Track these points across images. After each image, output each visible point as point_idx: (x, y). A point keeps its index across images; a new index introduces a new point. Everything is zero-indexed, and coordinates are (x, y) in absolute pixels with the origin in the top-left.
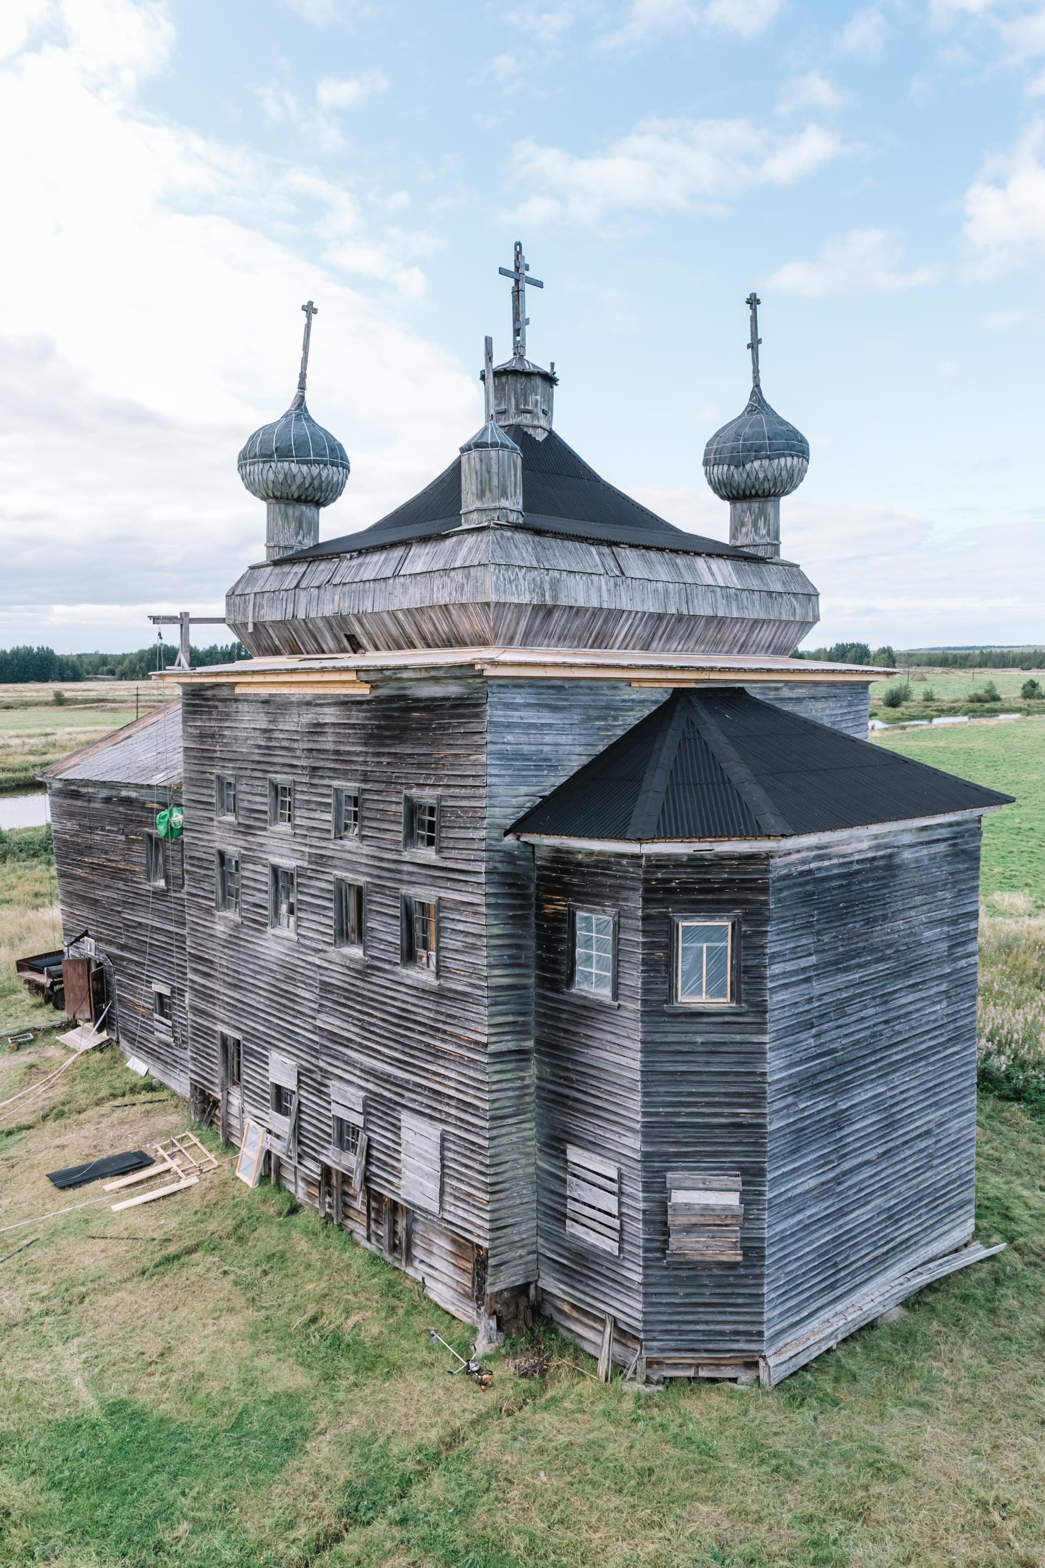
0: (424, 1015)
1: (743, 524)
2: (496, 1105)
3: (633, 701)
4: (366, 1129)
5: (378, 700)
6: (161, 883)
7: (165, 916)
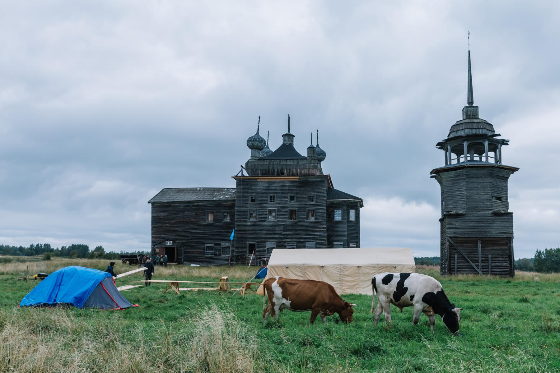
0: (311, 226)
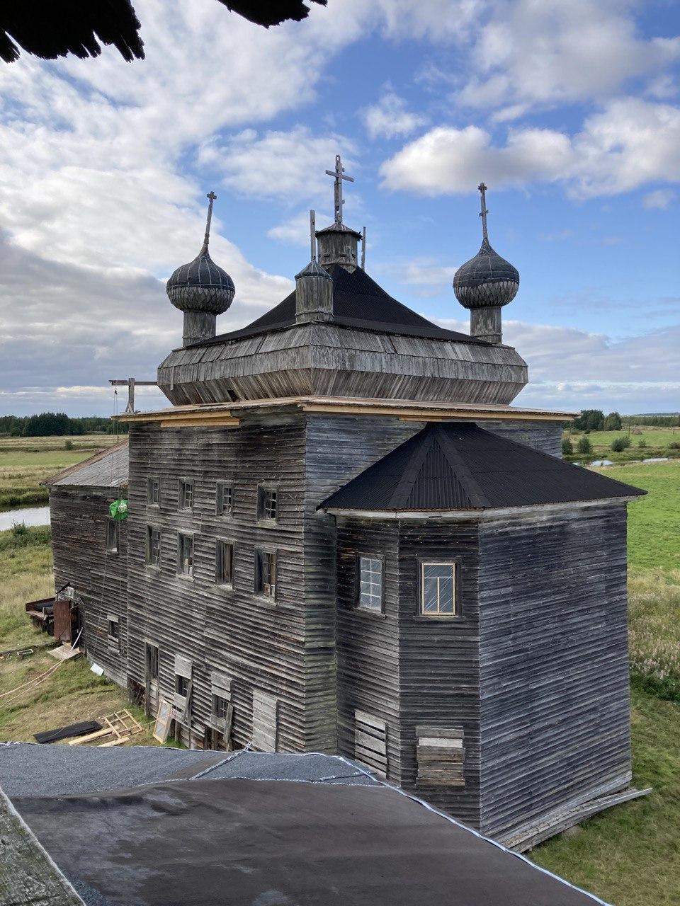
0: (268, 626)
1: (478, 323)
2: (310, 683)
3: (400, 429)
4: (232, 702)
5: (244, 428)
6: (115, 550)
7: (116, 572)
